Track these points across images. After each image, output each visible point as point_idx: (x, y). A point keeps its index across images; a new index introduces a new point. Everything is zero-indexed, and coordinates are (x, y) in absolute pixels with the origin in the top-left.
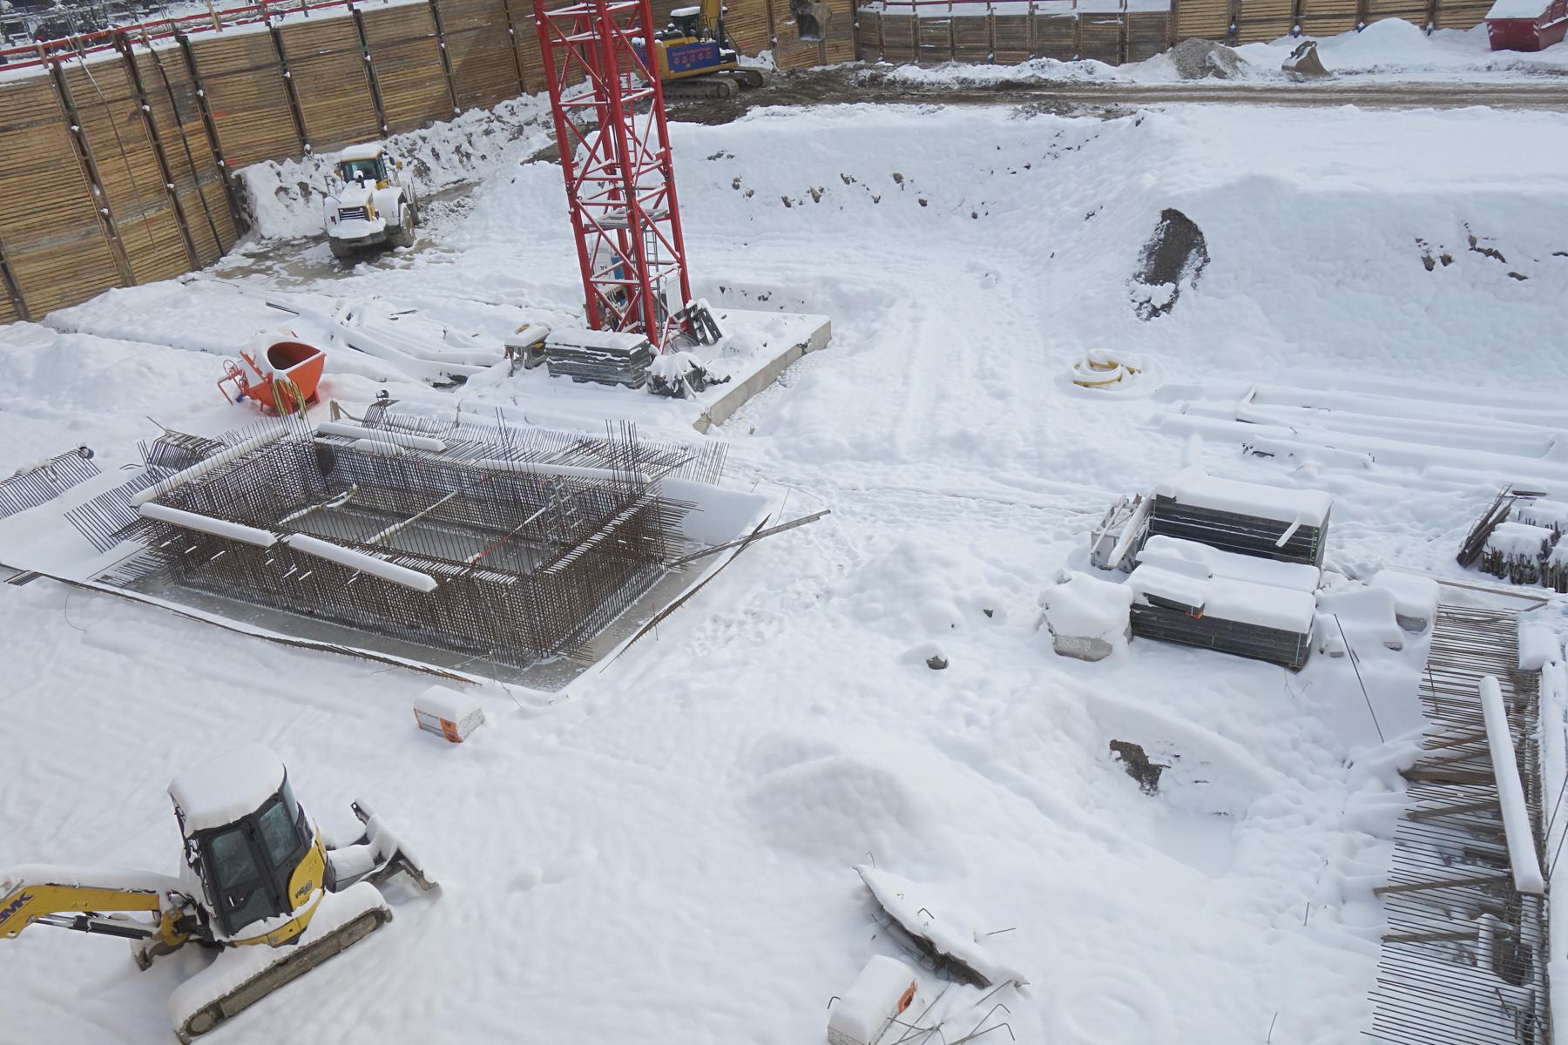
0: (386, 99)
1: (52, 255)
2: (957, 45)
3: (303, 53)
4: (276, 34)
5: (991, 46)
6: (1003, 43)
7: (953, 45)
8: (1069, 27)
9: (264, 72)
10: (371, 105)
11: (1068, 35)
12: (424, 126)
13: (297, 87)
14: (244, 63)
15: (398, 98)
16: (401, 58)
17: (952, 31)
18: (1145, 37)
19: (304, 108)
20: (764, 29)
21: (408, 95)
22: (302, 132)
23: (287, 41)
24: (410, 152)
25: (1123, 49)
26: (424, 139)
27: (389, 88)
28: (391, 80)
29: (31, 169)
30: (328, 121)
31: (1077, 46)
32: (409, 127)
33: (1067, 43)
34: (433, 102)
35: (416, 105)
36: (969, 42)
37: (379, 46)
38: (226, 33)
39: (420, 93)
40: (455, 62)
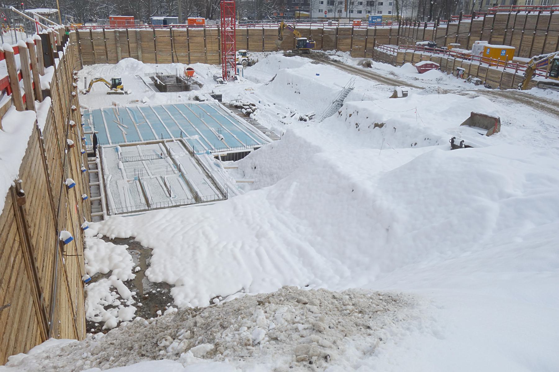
0: (265, 45)
1: (196, 57)
3: (251, 34)
4: (248, 30)
9: (244, 36)
10: (262, 46)
12: (271, 52)
13: (249, 40)
14: (241, 34)
15: (268, 45)
19: (249, 43)
20: (349, 47)
21: (269, 45)
22: (248, 47)
23: (249, 31)
24: (267, 56)
26: (270, 54)
27: (266, 43)
28: (267, 42)
29: (197, 43)
30: (253, 47)
32: (268, 51)
37: (265, 35)
38: (240, 28)
39: (272, 45)
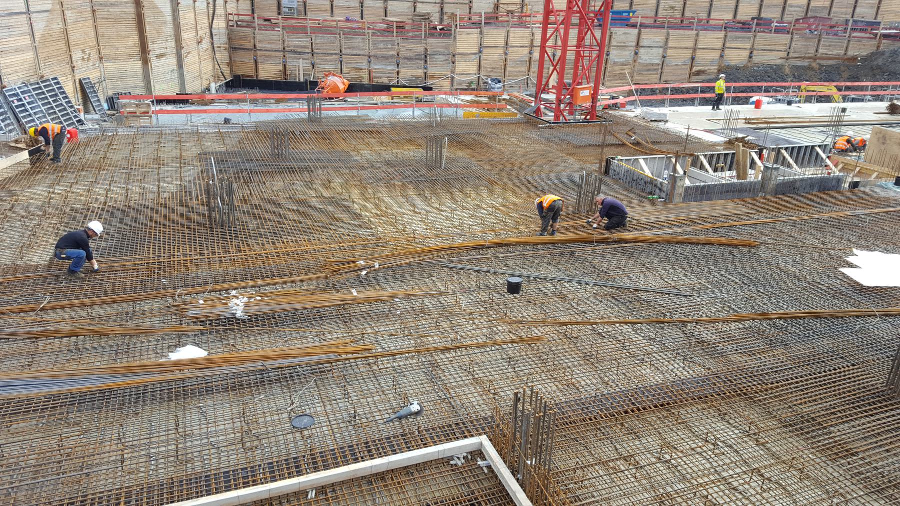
2: (315, 51)
5: (341, 51)
6: (348, 51)
7: (312, 51)
8: (394, 45)
11: (393, 49)
16: (9, 27)
17: (312, 43)
18: (438, 51)
25: (426, 57)
31: (398, 55)
33: (391, 53)
34: (28, 65)
35: (20, 67)
36: (326, 50)
40: (37, 35)
